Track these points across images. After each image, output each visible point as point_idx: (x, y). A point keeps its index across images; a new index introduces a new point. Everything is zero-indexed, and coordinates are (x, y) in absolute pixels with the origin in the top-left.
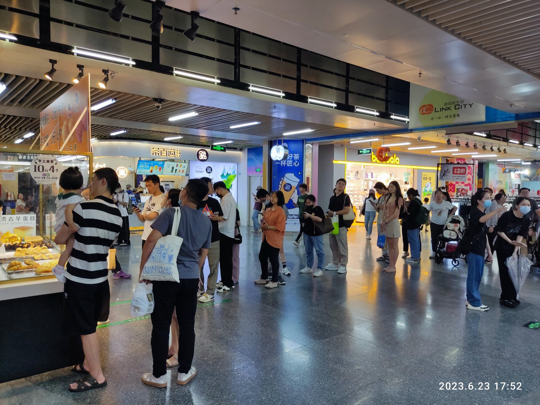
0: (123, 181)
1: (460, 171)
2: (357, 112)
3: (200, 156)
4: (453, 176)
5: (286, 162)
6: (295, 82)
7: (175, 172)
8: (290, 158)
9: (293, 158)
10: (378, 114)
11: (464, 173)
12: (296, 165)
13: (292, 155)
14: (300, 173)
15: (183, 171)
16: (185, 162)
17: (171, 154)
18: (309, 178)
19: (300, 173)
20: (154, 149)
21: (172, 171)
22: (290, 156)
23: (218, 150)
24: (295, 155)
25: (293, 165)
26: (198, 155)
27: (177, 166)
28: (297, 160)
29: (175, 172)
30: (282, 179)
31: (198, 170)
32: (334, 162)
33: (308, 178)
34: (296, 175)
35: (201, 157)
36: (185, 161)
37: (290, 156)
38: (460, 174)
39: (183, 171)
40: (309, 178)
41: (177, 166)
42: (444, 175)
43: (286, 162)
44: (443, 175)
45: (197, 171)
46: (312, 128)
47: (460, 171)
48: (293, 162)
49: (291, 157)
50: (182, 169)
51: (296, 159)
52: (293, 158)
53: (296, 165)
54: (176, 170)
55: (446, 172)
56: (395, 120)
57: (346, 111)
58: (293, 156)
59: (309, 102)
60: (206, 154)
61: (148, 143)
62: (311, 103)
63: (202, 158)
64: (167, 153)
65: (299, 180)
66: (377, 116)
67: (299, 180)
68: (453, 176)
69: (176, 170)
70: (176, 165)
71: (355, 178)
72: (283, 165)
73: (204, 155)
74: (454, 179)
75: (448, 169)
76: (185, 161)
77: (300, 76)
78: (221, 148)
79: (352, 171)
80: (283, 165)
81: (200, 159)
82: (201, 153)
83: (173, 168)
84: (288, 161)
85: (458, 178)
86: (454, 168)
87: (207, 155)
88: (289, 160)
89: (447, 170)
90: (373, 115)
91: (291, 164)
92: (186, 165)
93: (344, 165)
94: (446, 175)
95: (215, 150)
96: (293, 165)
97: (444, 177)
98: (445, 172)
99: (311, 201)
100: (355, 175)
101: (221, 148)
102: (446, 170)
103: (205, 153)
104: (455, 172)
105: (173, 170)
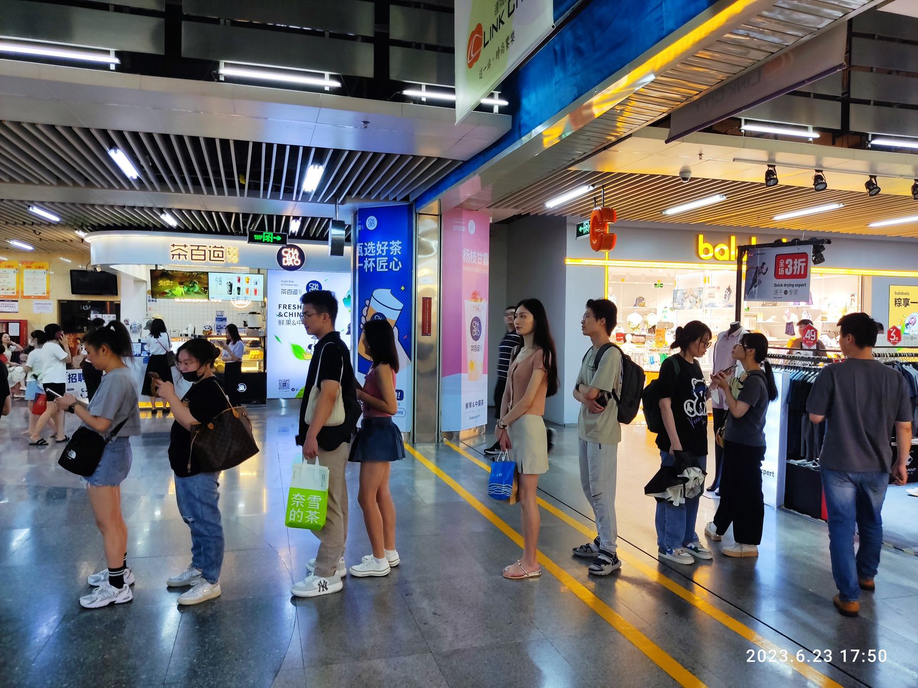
0: (243, 314)
1: (793, 265)
2: (748, 134)
3: (284, 259)
4: (776, 285)
5: (375, 262)
6: (839, 105)
7: (239, 294)
8: (382, 251)
9: (388, 251)
10: (337, 84)
11: (802, 273)
12: (396, 267)
13: (386, 243)
14: (403, 288)
15: (256, 291)
16: (259, 273)
17: (216, 255)
18: (430, 299)
19: (403, 288)
20: (176, 248)
21: (231, 291)
22: (383, 245)
23: (266, 242)
24: (393, 243)
25: (389, 269)
26: (280, 257)
27: (239, 281)
28: (397, 256)
29: (239, 294)
30: (367, 302)
31: (288, 288)
32: (568, 261)
33: (427, 302)
34: (396, 294)
35: (286, 262)
36: (259, 270)
37: (383, 245)
38: (792, 276)
39: (256, 291)
40: (430, 299)
41: (239, 281)
42: (755, 281)
43: (375, 262)
44: (751, 281)
45: (284, 291)
46: (839, 202)
47: (793, 265)
48: (388, 262)
49: (385, 248)
50: (252, 287)
51: (395, 254)
52: (388, 251)
53: (396, 267)
54: (239, 289)
55: (759, 274)
56: (430, 102)
57: (142, 73)
58: (389, 245)
59: (222, 79)
60: (298, 254)
61: (165, 235)
62: (228, 79)
63: (289, 263)
64: (205, 255)
65: (399, 305)
66: (334, 91)
67: (399, 305)
68: (776, 285)
69: (239, 289)
70: (236, 280)
71: (725, 304)
72: (369, 269)
73: (293, 257)
74: (779, 295)
75: (764, 264)
76: (259, 270)
77: (848, 92)
78: (275, 238)
79: (718, 288)
80: (369, 269)
81: (284, 264)
82: (286, 252)
83: (231, 286)
84: (378, 259)
85: (788, 289)
86: (779, 257)
87: (302, 256)
88: (380, 256)
89: (762, 267)
90: (320, 90)
91: (385, 264)
92: (260, 278)
93: (603, 268)
94: (760, 282)
95: (260, 241)
96: (389, 269)
97: (753, 289)
98: (756, 274)
99: (194, 360)
100: (725, 298)
101: (275, 238)
102: (759, 265)
103: (296, 252)
104: (781, 272)
105: (231, 288)
